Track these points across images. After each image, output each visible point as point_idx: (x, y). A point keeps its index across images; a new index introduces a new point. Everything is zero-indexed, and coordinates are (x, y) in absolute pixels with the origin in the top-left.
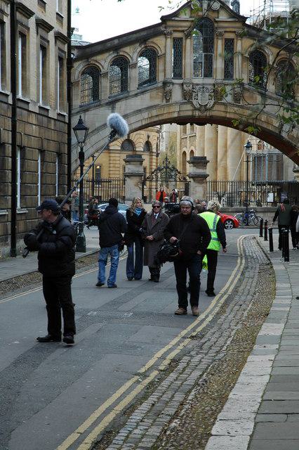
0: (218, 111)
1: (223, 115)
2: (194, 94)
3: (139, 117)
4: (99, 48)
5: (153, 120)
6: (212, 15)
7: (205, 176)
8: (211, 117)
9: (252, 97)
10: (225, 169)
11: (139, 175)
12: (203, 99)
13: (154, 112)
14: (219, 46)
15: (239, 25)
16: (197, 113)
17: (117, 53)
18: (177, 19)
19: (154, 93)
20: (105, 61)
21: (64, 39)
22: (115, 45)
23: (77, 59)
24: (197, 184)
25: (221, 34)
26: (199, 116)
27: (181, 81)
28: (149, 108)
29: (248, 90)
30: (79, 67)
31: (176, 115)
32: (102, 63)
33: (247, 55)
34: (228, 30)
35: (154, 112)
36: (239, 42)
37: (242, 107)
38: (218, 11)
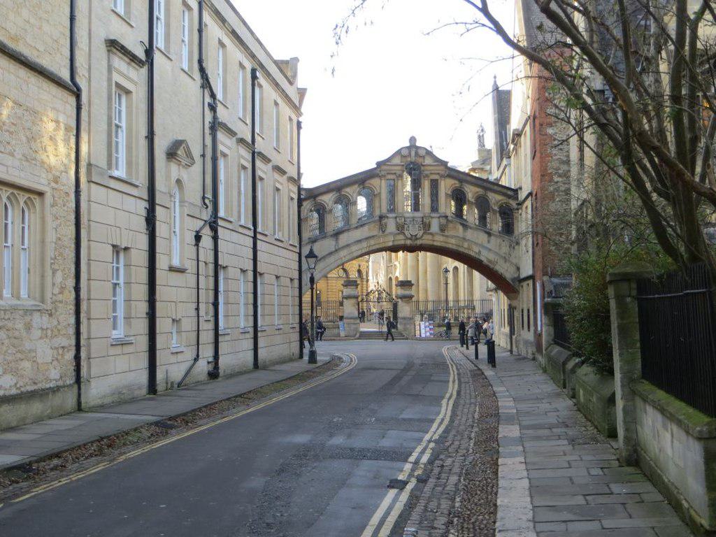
0: (427, 240)
1: (431, 243)
2: (406, 226)
5: (371, 249)
6: (420, 160)
7: (411, 297)
8: (421, 244)
9: (455, 227)
10: (426, 291)
11: (357, 297)
12: (413, 230)
14: (426, 185)
15: (442, 168)
16: (409, 242)
20: (328, 199)
21: (296, 181)
22: (339, 188)
23: (305, 199)
24: (404, 304)
25: (427, 176)
26: (411, 244)
27: (394, 215)
28: (367, 239)
29: (451, 222)
30: (307, 205)
34: (433, 172)
35: (372, 242)
36: (443, 183)
38: (424, 157)
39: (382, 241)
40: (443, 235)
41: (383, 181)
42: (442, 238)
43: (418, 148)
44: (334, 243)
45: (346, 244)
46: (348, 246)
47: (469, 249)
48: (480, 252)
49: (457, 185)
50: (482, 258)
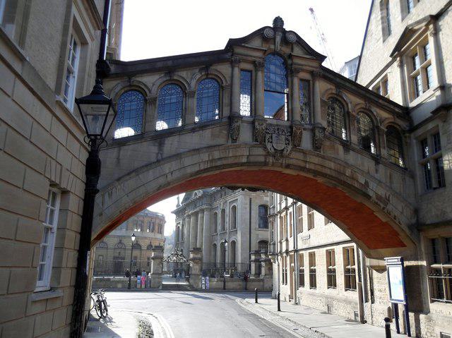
2: (268, 136)
3: (196, 159)
4: (147, 67)
9: (333, 147)
13: (217, 155)
15: (315, 64)
17: (170, 77)
18: (246, 45)
19: (217, 129)
20: (151, 81)
28: (210, 147)
29: (329, 139)
31: (244, 160)
32: (150, 85)
33: (325, 99)
35: (217, 155)
37: (323, 157)
39: (231, 155)
40: (318, 156)
41: (236, 70)
42: (316, 160)
43: (284, 32)
44: (154, 149)
45: (174, 153)
46: (178, 156)
47: (353, 178)
48: (366, 183)
49: (334, 92)
50: (371, 194)
